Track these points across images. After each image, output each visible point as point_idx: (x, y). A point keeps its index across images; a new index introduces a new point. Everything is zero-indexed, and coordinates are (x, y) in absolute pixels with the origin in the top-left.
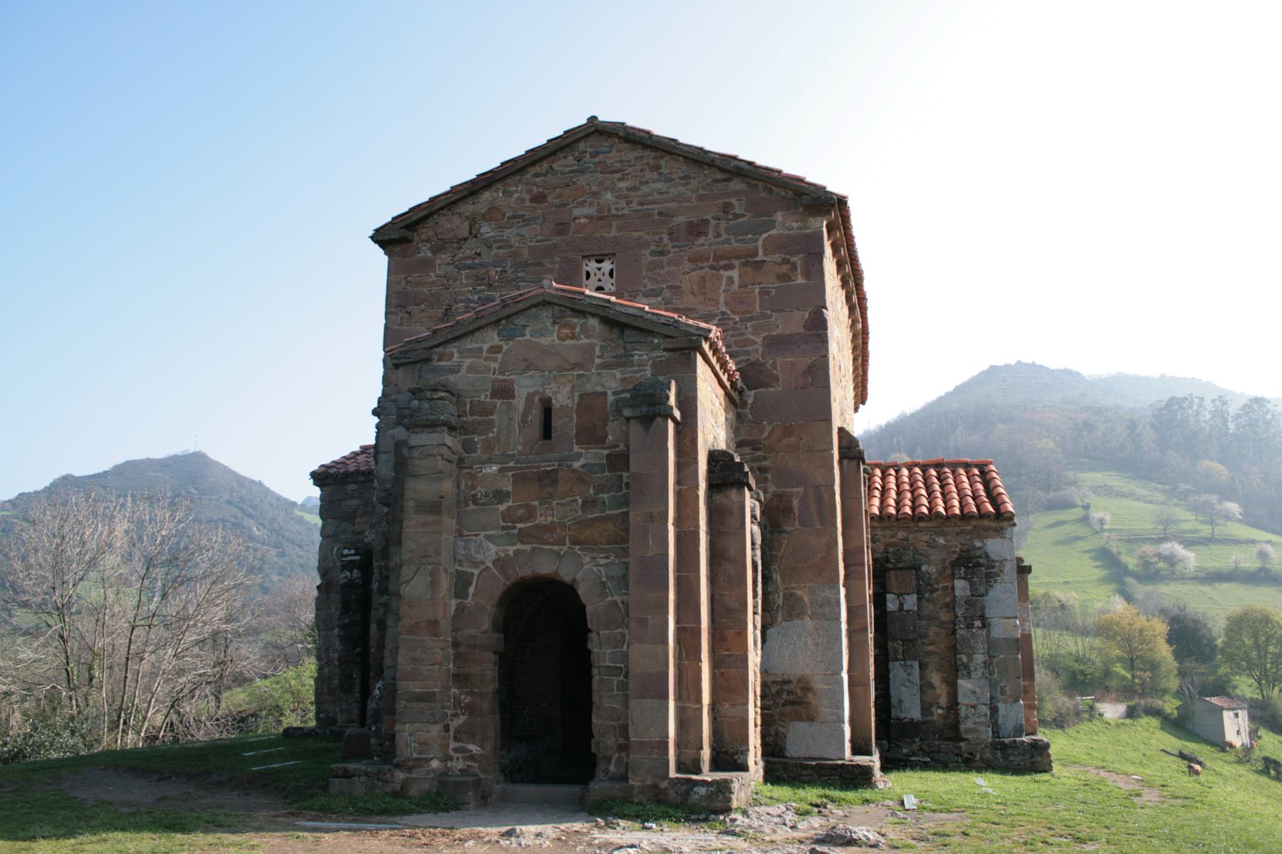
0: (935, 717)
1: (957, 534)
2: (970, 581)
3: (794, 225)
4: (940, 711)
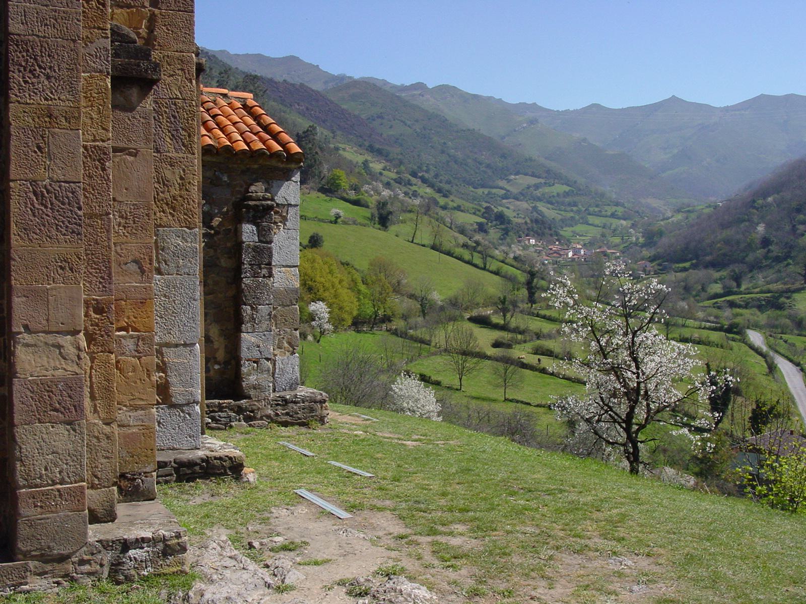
1: (243, 172)
2: (257, 225)
4: (217, 367)
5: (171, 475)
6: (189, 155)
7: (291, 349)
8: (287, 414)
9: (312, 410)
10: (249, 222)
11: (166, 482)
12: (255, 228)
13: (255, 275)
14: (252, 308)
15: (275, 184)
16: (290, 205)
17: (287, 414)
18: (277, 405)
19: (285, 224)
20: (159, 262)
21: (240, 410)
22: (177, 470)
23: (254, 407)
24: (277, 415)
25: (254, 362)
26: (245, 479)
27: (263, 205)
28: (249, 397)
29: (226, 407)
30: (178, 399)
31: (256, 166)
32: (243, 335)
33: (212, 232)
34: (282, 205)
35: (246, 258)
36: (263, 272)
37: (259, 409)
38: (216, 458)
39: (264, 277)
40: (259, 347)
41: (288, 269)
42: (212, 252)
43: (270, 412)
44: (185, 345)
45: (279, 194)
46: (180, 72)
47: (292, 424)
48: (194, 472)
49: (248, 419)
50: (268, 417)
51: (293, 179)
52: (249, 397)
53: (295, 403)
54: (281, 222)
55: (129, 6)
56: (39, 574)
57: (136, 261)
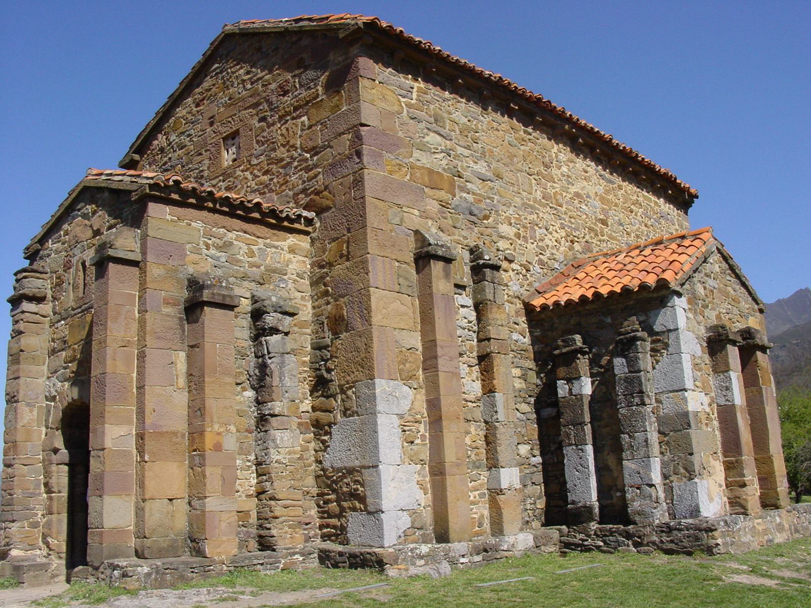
0: (615, 501)
2: (625, 357)
3: (340, 59)
5: (346, 562)
6: (369, 327)
7: (688, 475)
8: (672, 541)
9: (697, 539)
10: (618, 356)
11: (344, 567)
12: (624, 360)
13: (630, 405)
14: (630, 437)
15: (652, 314)
16: (669, 331)
17: (672, 541)
18: (662, 532)
19: (668, 350)
20: (357, 408)
21: (628, 536)
22: (348, 558)
23: (641, 533)
24: (662, 542)
25: (638, 488)
26: (386, 573)
27: (626, 338)
28: (634, 523)
29: (615, 532)
30: (371, 508)
31: (631, 303)
32: (624, 462)
33: (603, 370)
34: (662, 332)
35: (620, 390)
36: (636, 401)
37: (644, 535)
38: (368, 553)
39: (637, 405)
40: (639, 473)
41: (676, 393)
42: (604, 388)
43: (655, 538)
44: (373, 467)
45: (657, 323)
46: (362, 271)
47: (678, 553)
48: (357, 563)
49: (636, 545)
50: (654, 543)
51: (669, 304)
52: (634, 523)
53: (680, 530)
54: (663, 349)
55: (337, 239)
56: (93, 575)
57: (199, 409)
